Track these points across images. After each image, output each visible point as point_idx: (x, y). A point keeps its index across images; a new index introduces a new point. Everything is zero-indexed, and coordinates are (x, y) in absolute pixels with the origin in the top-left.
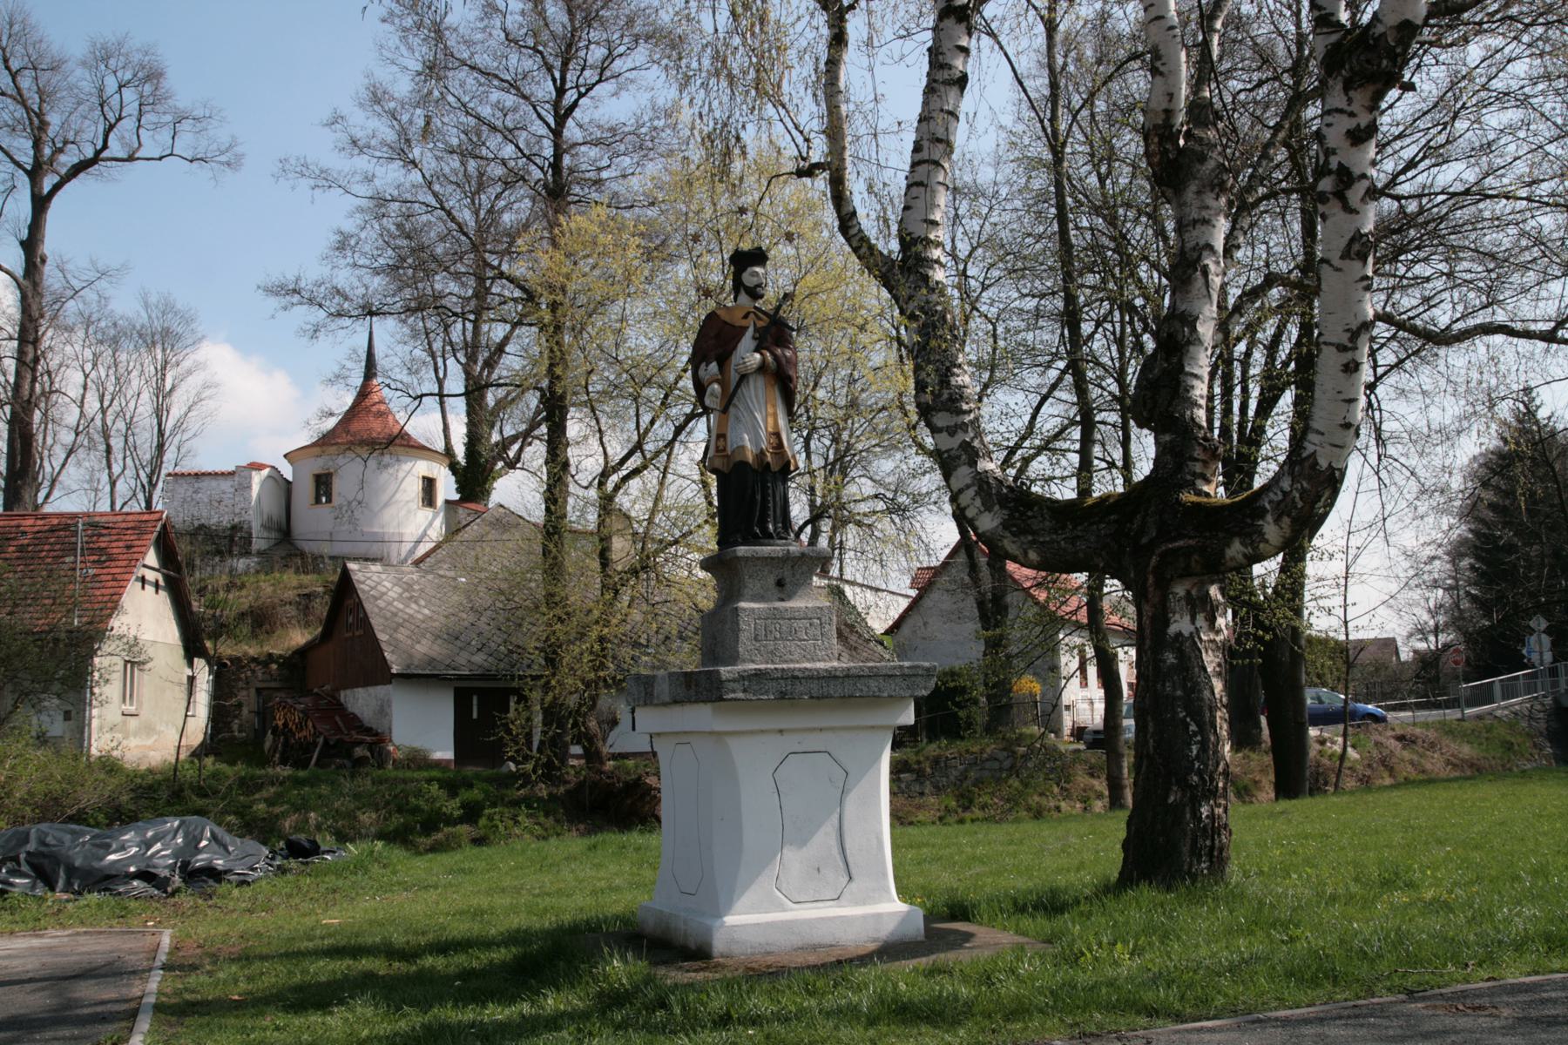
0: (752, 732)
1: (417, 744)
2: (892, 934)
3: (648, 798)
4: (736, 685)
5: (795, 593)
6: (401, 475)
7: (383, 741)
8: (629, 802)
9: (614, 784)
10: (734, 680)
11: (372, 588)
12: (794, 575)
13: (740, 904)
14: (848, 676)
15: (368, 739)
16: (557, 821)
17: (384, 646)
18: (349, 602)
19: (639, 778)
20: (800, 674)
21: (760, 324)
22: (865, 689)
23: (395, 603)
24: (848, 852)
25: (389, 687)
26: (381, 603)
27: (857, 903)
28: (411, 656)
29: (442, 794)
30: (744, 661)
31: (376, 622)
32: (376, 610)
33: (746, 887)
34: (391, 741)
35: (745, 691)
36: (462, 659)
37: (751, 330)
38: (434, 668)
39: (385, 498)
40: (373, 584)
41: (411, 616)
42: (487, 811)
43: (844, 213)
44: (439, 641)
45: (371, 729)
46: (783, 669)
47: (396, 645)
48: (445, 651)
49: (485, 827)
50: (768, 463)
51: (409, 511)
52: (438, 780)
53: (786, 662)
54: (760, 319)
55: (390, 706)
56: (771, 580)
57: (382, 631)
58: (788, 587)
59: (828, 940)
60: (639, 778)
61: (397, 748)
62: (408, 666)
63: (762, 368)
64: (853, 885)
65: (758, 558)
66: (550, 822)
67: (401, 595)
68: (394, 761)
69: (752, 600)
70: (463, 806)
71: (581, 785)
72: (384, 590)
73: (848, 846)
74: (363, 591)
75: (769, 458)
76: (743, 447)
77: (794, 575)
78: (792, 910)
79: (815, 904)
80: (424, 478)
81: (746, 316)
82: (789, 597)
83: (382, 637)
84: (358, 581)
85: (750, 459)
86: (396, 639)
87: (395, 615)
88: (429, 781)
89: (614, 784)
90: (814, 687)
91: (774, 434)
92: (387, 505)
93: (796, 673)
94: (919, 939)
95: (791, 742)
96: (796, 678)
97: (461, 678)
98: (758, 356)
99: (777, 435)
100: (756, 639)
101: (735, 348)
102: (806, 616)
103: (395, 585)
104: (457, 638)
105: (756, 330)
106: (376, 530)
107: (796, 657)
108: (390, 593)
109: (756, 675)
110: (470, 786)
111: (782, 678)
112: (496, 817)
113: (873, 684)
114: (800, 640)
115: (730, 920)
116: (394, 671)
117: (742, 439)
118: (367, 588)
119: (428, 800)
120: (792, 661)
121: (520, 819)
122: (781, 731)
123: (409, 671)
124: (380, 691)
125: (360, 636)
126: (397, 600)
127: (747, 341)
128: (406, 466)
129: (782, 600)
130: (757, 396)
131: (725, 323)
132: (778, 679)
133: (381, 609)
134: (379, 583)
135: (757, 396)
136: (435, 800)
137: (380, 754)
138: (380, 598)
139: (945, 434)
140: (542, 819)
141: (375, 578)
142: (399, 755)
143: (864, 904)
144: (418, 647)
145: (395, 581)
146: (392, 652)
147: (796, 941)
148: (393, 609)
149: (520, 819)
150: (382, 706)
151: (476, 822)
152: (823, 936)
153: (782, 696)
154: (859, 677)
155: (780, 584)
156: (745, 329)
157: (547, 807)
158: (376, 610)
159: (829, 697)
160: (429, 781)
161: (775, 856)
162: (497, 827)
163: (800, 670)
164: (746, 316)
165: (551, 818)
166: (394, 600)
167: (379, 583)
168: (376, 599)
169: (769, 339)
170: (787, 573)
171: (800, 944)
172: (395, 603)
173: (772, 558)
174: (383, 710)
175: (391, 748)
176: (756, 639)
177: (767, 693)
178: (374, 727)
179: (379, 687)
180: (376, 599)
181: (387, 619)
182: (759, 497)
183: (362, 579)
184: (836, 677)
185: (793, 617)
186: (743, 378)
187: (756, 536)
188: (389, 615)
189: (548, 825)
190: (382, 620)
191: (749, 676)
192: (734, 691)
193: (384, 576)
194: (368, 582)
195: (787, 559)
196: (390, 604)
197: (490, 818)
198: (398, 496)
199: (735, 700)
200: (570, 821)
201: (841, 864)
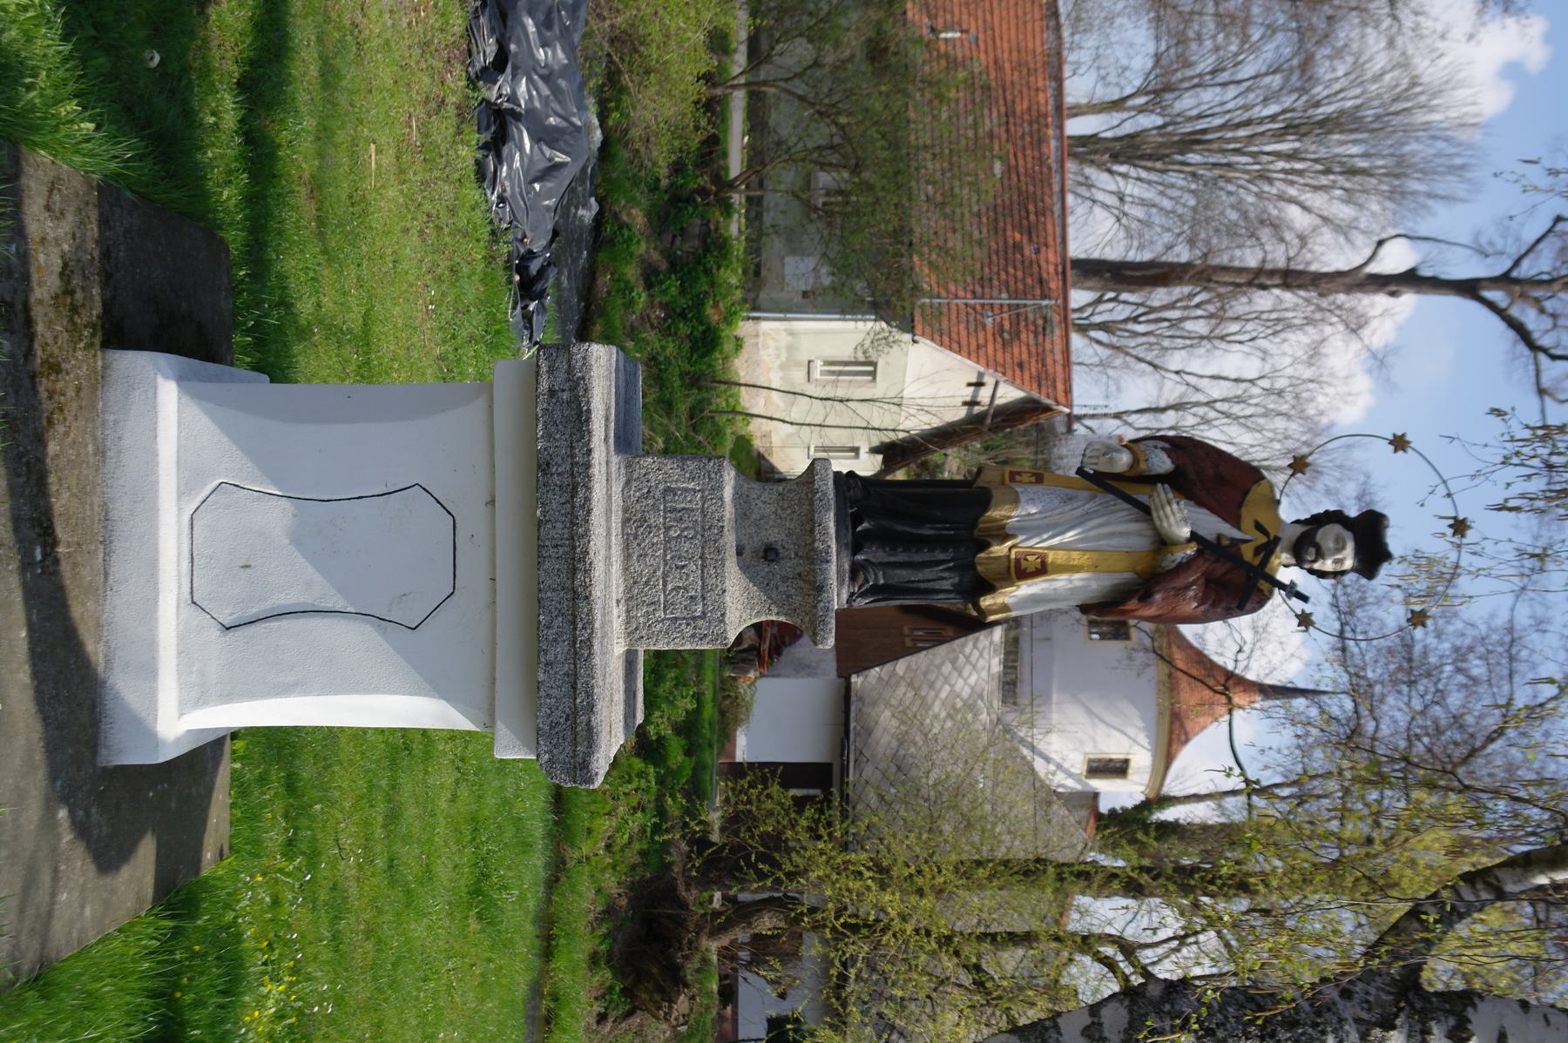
0: (492, 446)
1: (757, 710)
2: (117, 697)
3: (657, 997)
4: (561, 375)
5: (752, 579)
6: (1131, 731)
7: (761, 665)
8: (655, 971)
9: (680, 949)
10: (570, 370)
11: (967, 658)
12: (785, 579)
13: (196, 412)
14: (575, 596)
15: (765, 647)
16: (633, 868)
17: (888, 667)
18: (950, 631)
19: (686, 985)
20: (578, 500)
21: (1247, 553)
22: (551, 634)
23: (947, 688)
24: (274, 624)
25: (833, 674)
26: (947, 668)
27: (182, 638)
28: (874, 703)
29: (680, 715)
30: (628, 466)
31: (921, 660)
32: (938, 661)
33: (224, 427)
34: (762, 676)
35: (552, 392)
36: (868, 771)
37: (1236, 534)
38: (857, 734)
39: (1098, 710)
40: (973, 659)
41: (929, 708)
42: (651, 769)
43: (1499, 873)
44: (894, 744)
45: (779, 654)
46: (588, 466)
47: (890, 683)
48: (880, 750)
49: (630, 766)
50: (985, 546)
51: (1081, 742)
52: (698, 711)
53: (627, 547)
54: (1257, 550)
55: (809, 675)
56: (775, 536)
57: (909, 667)
58: (765, 568)
59: (118, 570)
60: (686, 985)
61: (753, 683)
62: (861, 699)
63: (1163, 543)
64: (215, 632)
65: (811, 503)
66: (632, 856)
67: (958, 696)
68: (734, 679)
69: (738, 496)
70: (661, 739)
71: (683, 905)
72: (965, 674)
73: (284, 623)
74: (963, 646)
75: (999, 550)
76: (1016, 501)
77: (785, 579)
78: (180, 509)
79: (186, 555)
80: (1126, 761)
81: (1259, 527)
82: (745, 568)
83: (901, 666)
84: (977, 640)
85: (994, 513)
86: (897, 685)
87: (931, 686)
88: (698, 697)
89: (680, 949)
90: (559, 530)
91: (1043, 563)
92: (1090, 712)
93: (581, 493)
94: (103, 752)
95: (473, 520)
96: (574, 493)
97: (844, 770)
98: (1185, 532)
99: (1042, 570)
100: (667, 490)
101: (1200, 503)
102: (709, 593)
103: (972, 688)
104: (899, 768)
105: (1236, 543)
106: (1055, 697)
107: (636, 566)
108: (960, 683)
109: (580, 413)
110: (688, 753)
111: (573, 464)
112: (643, 784)
113: (561, 649)
114: (665, 576)
115: (168, 393)
116: (854, 679)
117: (1031, 501)
118: (967, 650)
119: (671, 693)
120: (627, 557)
121: (639, 814)
122: (492, 502)
123: (853, 698)
124: (831, 666)
125: (904, 642)
126: (952, 691)
127: (1213, 525)
128: (1143, 739)
129: (739, 553)
130: (1112, 535)
131: (1246, 493)
132: (572, 456)
133: (939, 667)
134: (974, 667)
135: (1112, 535)
136: (671, 703)
137: (743, 661)
138: (954, 668)
139: (1088, 1020)
140: (637, 846)
141: (982, 663)
142: (743, 686)
143: (180, 653)
144: (887, 713)
145: (978, 689)
146: (880, 679)
147: (120, 510)
148: (939, 684)
149: (639, 814)
150: (809, 667)
151: (638, 755)
152: (123, 567)
153: (544, 467)
154: (574, 623)
155: (769, 553)
156: (1237, 524)
157: (655, 854)
158: (938, 661)
159: (540, 559)
160: (698, 697)
161: (277, 485)
162: (629, 782)
163: (588, 499)
164: (1259, 527)
165: (638, 859)
166: (952, 686)
167: (974, 667)
168: (954, 662)
169: (1220, 569)
170: (788, 566)
171: (114, 515)
172: (947, 688)
173: (812, 531)
174: (803, 668)
175: (752, 675)
176: (667, 490)
177: (548, 436)
178: (783, 658)
179: (834, 664)
180: (954, 662)
181: (925, 674)
182: (927, 531)
183: (980, 646)
184: (573, 571)
185: (709, 561)
186: (1145, 510)
187: (857, 520)
188: (932, 677)
189: (628, 854)
190: (923, 667)
191: (577, 398)
192: (551, 370)
193: (984, 674)
194: (976, 653)
195: (813, 558)
196: (947, 680)
197: (642, 775)
198: (1102, 726)
199: (538, 374)
200: (632, 887)
201: (253, 611)
